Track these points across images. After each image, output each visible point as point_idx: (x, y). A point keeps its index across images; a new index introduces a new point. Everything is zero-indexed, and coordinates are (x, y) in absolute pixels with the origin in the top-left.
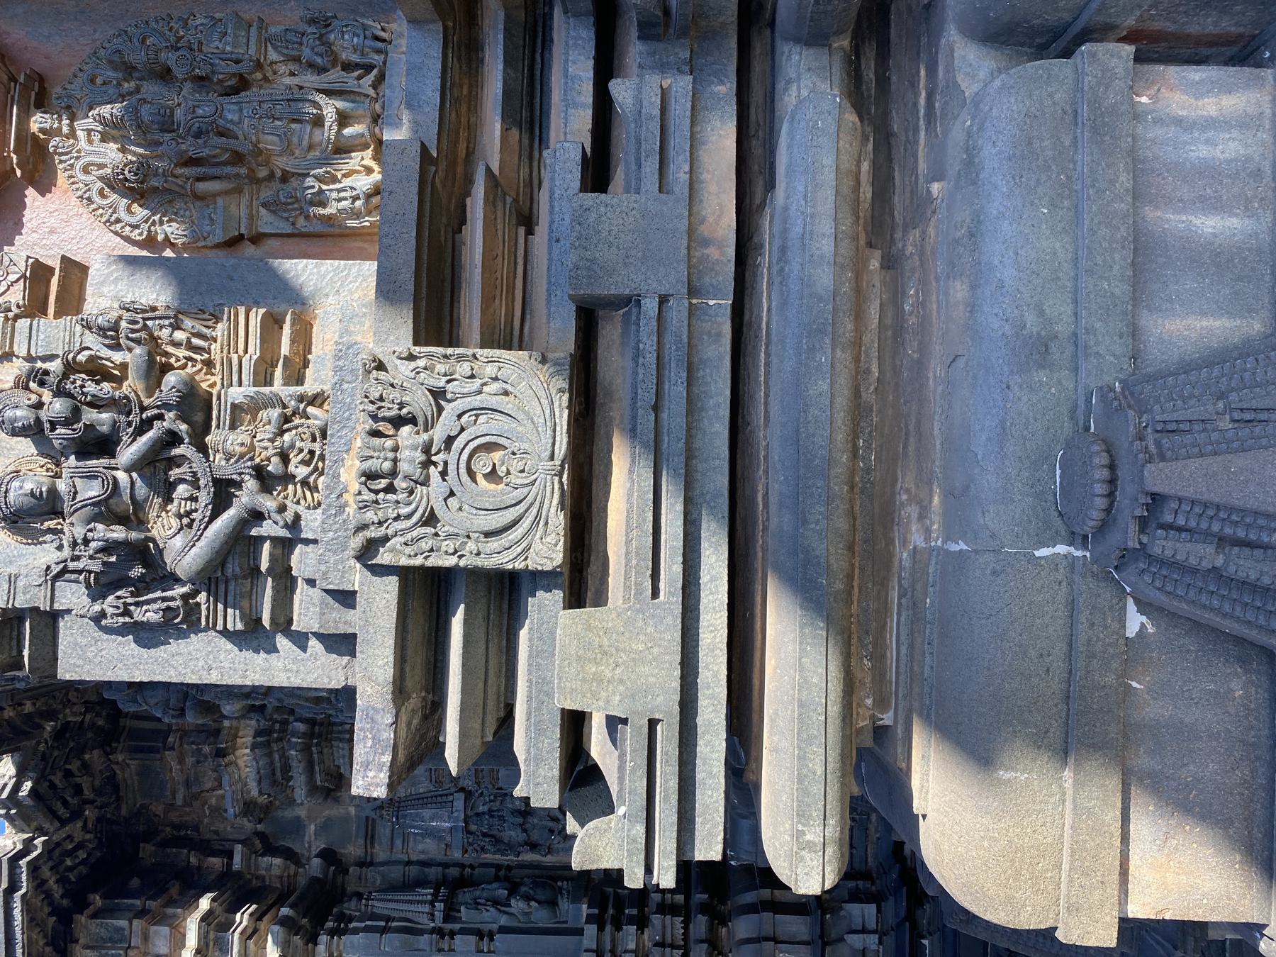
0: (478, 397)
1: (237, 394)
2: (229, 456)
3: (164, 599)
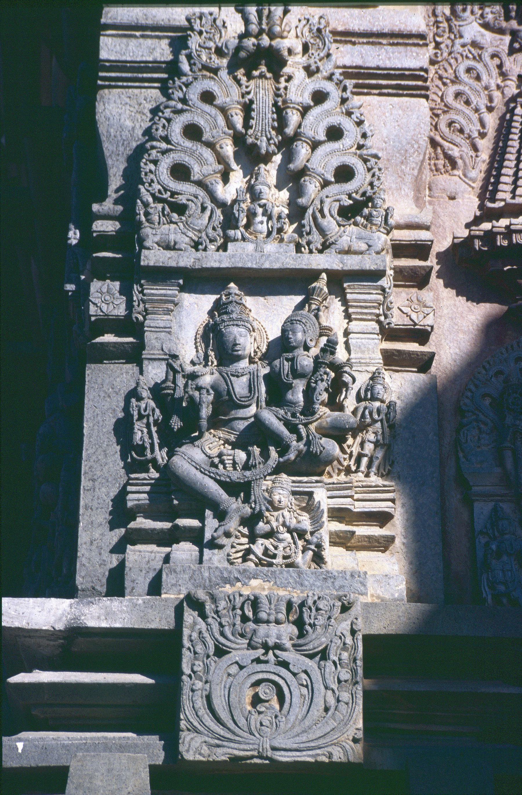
0: (322, 687)
1: (321, 495)
2: (270, 491)
3: (152, 445)
